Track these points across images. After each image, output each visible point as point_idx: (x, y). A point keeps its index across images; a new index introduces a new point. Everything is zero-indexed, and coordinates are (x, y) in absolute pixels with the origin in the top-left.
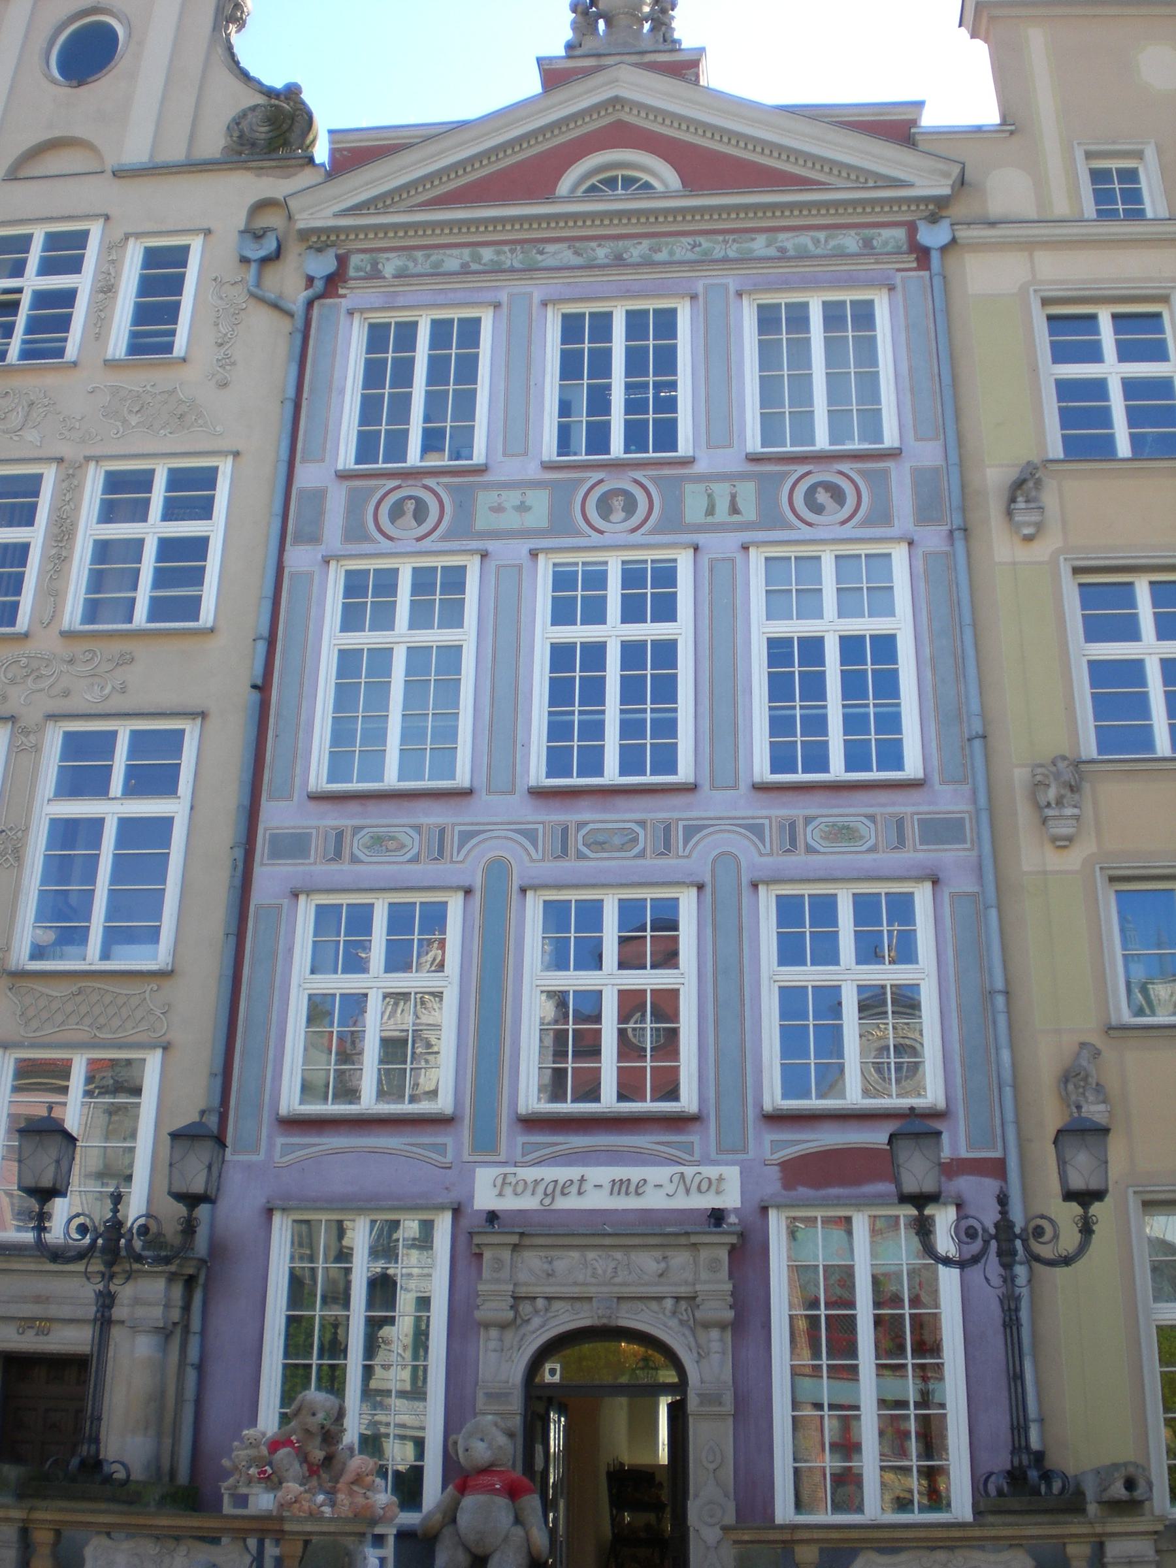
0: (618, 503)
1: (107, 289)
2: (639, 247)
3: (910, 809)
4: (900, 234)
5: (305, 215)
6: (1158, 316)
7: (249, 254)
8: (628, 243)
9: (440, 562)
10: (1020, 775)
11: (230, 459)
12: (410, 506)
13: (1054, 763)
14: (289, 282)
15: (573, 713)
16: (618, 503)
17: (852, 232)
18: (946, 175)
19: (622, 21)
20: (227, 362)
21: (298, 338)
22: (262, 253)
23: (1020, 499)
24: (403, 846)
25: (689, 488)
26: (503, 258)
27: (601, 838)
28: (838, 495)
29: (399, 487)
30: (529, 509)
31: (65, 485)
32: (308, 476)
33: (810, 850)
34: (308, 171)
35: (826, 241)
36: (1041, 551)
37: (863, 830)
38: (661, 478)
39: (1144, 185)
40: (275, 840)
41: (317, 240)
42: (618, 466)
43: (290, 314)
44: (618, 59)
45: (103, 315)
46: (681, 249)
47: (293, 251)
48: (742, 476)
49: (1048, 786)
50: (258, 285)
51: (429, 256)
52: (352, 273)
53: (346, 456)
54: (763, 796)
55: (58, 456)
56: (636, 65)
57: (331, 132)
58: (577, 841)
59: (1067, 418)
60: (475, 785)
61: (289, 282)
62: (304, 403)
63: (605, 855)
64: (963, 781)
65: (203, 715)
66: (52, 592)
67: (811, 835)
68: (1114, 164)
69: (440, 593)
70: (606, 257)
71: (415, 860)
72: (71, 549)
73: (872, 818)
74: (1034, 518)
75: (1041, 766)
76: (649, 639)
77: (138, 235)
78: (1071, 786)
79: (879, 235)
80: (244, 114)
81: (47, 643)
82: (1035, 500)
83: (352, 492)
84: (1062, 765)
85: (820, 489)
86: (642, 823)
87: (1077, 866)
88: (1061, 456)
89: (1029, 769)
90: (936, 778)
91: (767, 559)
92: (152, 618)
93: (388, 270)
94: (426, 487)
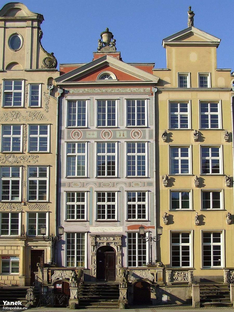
0: (107, 134)
12: (77, 133)
16: (107, 134)
20: (47, 108)
22: (51, 89)
23: (163, 136)
24: (78, 185)
25: (117, 132)
30: (94, 134)
58: (102, 185)
71: (80, 187)
73: (141, 182)
86: (110, 182)
94: (79, 130)
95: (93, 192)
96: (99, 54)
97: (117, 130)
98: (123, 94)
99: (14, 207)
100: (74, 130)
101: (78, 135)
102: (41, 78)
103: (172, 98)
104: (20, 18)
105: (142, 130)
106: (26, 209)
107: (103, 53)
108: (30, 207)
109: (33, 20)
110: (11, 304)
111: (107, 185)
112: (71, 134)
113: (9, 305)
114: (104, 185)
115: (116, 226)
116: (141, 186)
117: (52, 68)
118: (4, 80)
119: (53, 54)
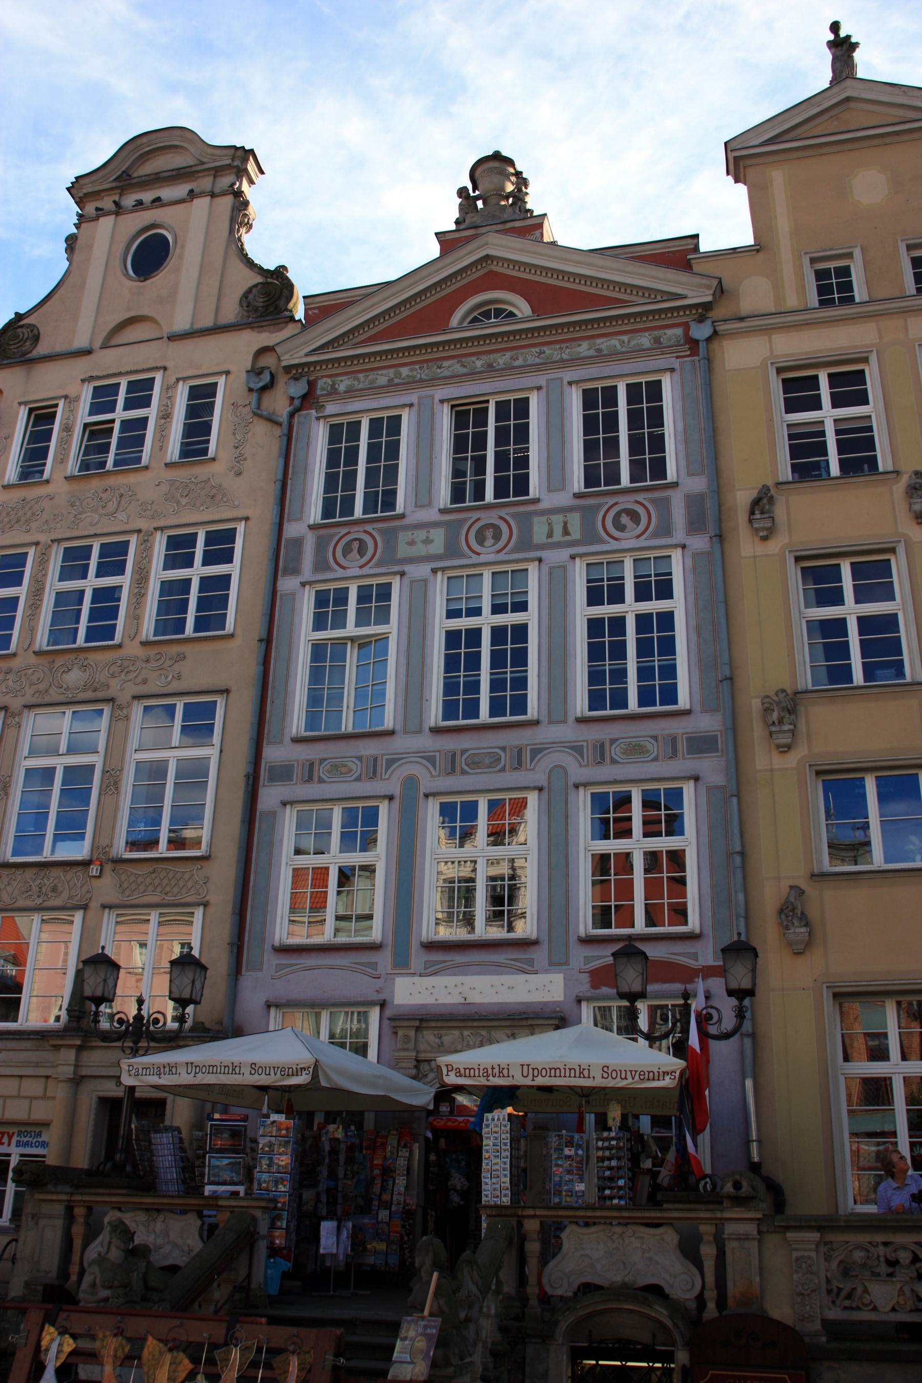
0: (489, 533)
1: (165, 416)
2: (504, 358)
3: (681, 731)
4: (679, 331)
5: (287, 357)
6: (863, 371)
7: (252, 386)
8: (498, 355)
9: (374, 581)
10: (756, 704)
11: (243, 523)
12: (356, 545)
13: (776, 694)
14: (279, 402)
15: (460, 676)
16: (489, 533)
17: (647, 334)
18: (708, 287)
19: (493, 201)
20: (240, 458)
21: (285, 438)
22: (261, 384)
23: (757, 512)
24: (351, 770)
25: (536, 520)
26: (415, 373)
27: (477, 760)
28: (635, 517)
29: (349, 533)
30: (432, 541)
31: (142, 547)
32: (292, 530)
34: (290, 326)
35: (629, 342)
36: (774, 546)
37: (649, 747)
38: (518, 514)
39: (854, 278)
40: (271, 769)
41: (295, 371)
42: (490, 507)
43: (279, 424)
44: (488, 228)
45: (164, 433)
46: (531, 356)
47: (282, 380)
48: (571, 509)
49: (773, 710)
50: (259, 407)
51: (367, 376)
52: (319, 392)
53: (314, 512)
54: (583, 726)
55: (138, 528)
56: (497, 232)
57: (304, 297)
58: (461, 762)
59: (795, 452)
60: (396, 728)
61: (279, 402)
62: (289, 482)
63: (479, 771)
64: (718, 710)
65: (227, 691)
66: (135, 617)
67: (615, 751)
68: (831, 265)
69: (375, 600)
71: (358, 779)
72: (147, 588)
73: (655, 738)
74: (768, 524)
75: (768, 697)
76: (509, 624)
77: (184, 379)
78: (788, 710)
79: (665, 334)
80: (250, 290)
81: (133, 649)
82: (769, 511)
84: (782, 696)
85: (623, 515)
86: (503, 749)
87: (794, 765)
88: (790, 479)
89: (759, 700)
90: (697, 708)
91: (588, 564)
92: (196, 630)
93: (342, 388)
94: (365, 532)
98: (563, 364)
99: (54, 890)
100: (344, 531)
101: (362, 551)
103: (787, 356)
105: (652, 501)
108: (125, 885)
114: (474, 763)
115: (528, 969)
116: (655, 759)
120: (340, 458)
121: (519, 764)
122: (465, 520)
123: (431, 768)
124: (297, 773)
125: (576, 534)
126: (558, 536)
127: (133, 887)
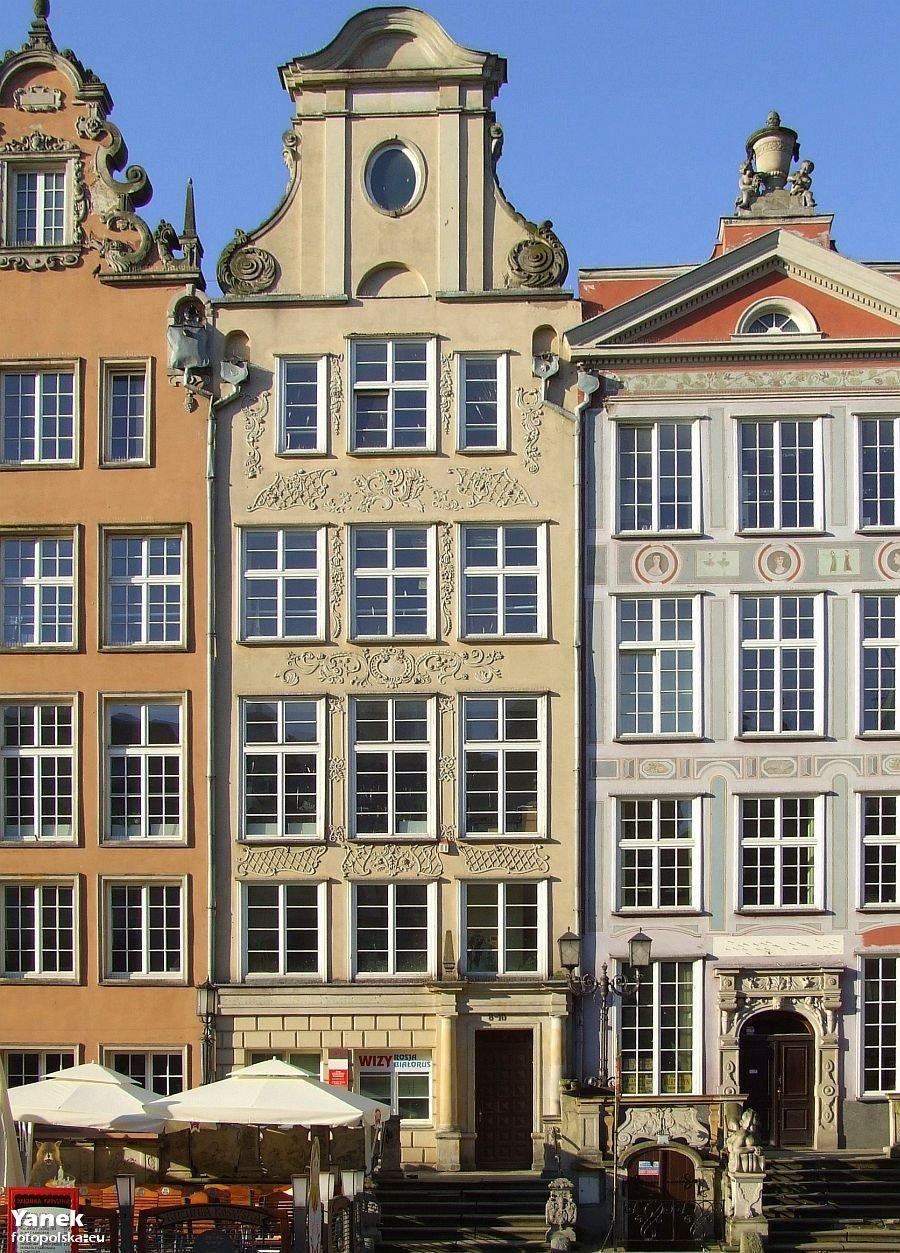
0: (780, 561)
12: (657, 559)
16: (780, 561)
20: (536, 454)
22: (550, 373)
27: (773, 766)
30: (728, 563)
33: (884, 773)
48: (851, 545)
51: (655, 377)
67: (885, 765)
70: (769, 383)
71: (674, 777)
83: (621, 548)
86: (795, 758)
94: (665, 547)
95: (725, 800)
96: (743, 223)
97: (820, 545)
98: (846, 393)
99: (407, 862)
100: (645, 543)
101: (663, 566)
102: (505, 328)
104: (414, 73)
106: (457, 867)
107: (761, 218)
108: (474, 860)
109: (464, 83)
110: (42, 1224)
111: (779, 771)
112: (634, 561)
113: (35, 1224)
114: (771, 768)
117: (549, 286)
118: (353, 338)
119: (548, 224)
120: (629, 465)
121: (809, 772)
122: (759, 545)
123: (736, 772)
124: (619, 769)
125: (856, 570)
126: (840, 569)
127: (481, 861)
